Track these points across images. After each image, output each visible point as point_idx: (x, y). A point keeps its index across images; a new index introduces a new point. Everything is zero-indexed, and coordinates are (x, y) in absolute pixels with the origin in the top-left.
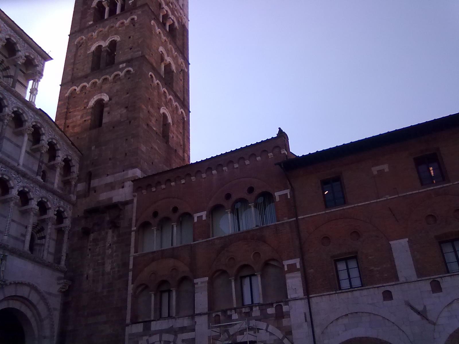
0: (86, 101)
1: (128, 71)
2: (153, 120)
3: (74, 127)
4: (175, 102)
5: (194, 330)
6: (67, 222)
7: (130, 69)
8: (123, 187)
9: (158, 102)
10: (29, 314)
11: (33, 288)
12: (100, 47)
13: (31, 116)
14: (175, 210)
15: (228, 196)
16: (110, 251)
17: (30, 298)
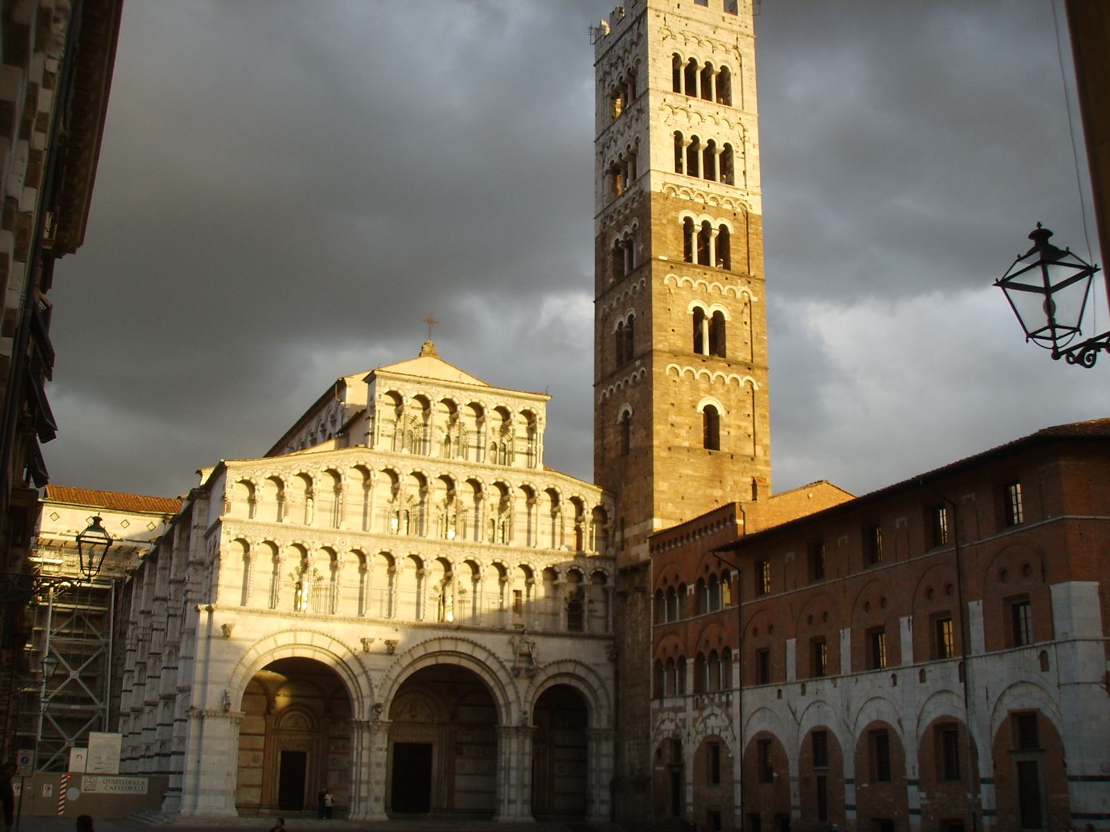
0: (616, 412)
1: (643, 372)
2: (683, 432)
3: (610, 450)
4: (727, 376)
5: (685, 711)
6: (610, 582)
7: (644, 369)
8: (645, 542)
9: (691, 399)
10: (581, 687)
11: (576, 662)
12: (621, 324)
13: (539, 483)
14: (677, 577)
15: (707, 567)
16: (640, 619)
17: (576, 672)
